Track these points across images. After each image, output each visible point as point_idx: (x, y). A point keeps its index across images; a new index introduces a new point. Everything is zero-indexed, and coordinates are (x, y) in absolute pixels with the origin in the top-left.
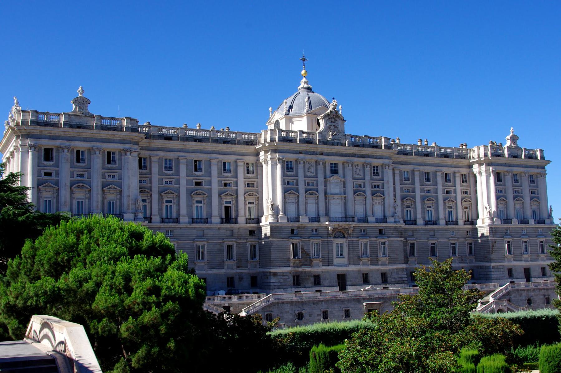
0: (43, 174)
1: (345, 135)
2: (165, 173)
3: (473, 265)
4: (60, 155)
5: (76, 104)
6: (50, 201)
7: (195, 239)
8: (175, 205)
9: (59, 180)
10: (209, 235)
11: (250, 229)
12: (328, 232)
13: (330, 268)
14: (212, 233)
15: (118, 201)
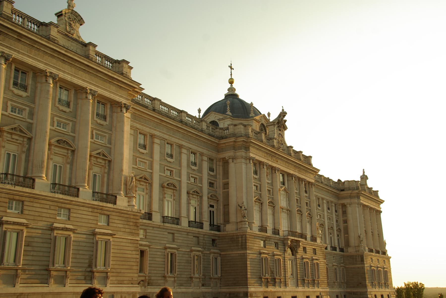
0: (9, 109)
1: (288, 147)
2: (139, 150)
3: (346, 290)
4: (39, 85)
5: (66, 19)
6: (15, 156)
7: (167, 245)
8: (147, 197)
9: (32, 124)
10: (179, 241)
11: (213, 238)
12: (285, 248)
13: (288, 289)
14: (182, 238)
15: (106, 175)
